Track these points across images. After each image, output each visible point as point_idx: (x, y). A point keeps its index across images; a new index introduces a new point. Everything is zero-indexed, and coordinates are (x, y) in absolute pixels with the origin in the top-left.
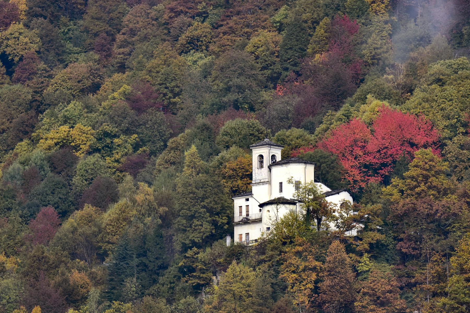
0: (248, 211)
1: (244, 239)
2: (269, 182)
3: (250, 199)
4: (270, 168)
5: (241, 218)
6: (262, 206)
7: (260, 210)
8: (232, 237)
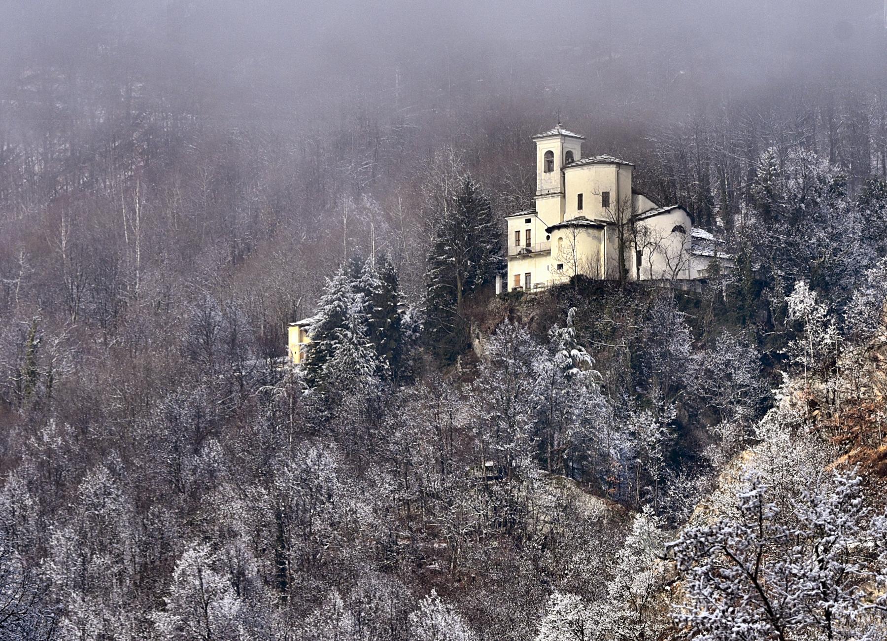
0: (528, 239)
1: (522, 283)
2: (563, 194)
3: (533, 219)
4: (563, 170)
5: (519, 249)
6: (549, 230)
7: (548, 238)
8: (504, 276)
